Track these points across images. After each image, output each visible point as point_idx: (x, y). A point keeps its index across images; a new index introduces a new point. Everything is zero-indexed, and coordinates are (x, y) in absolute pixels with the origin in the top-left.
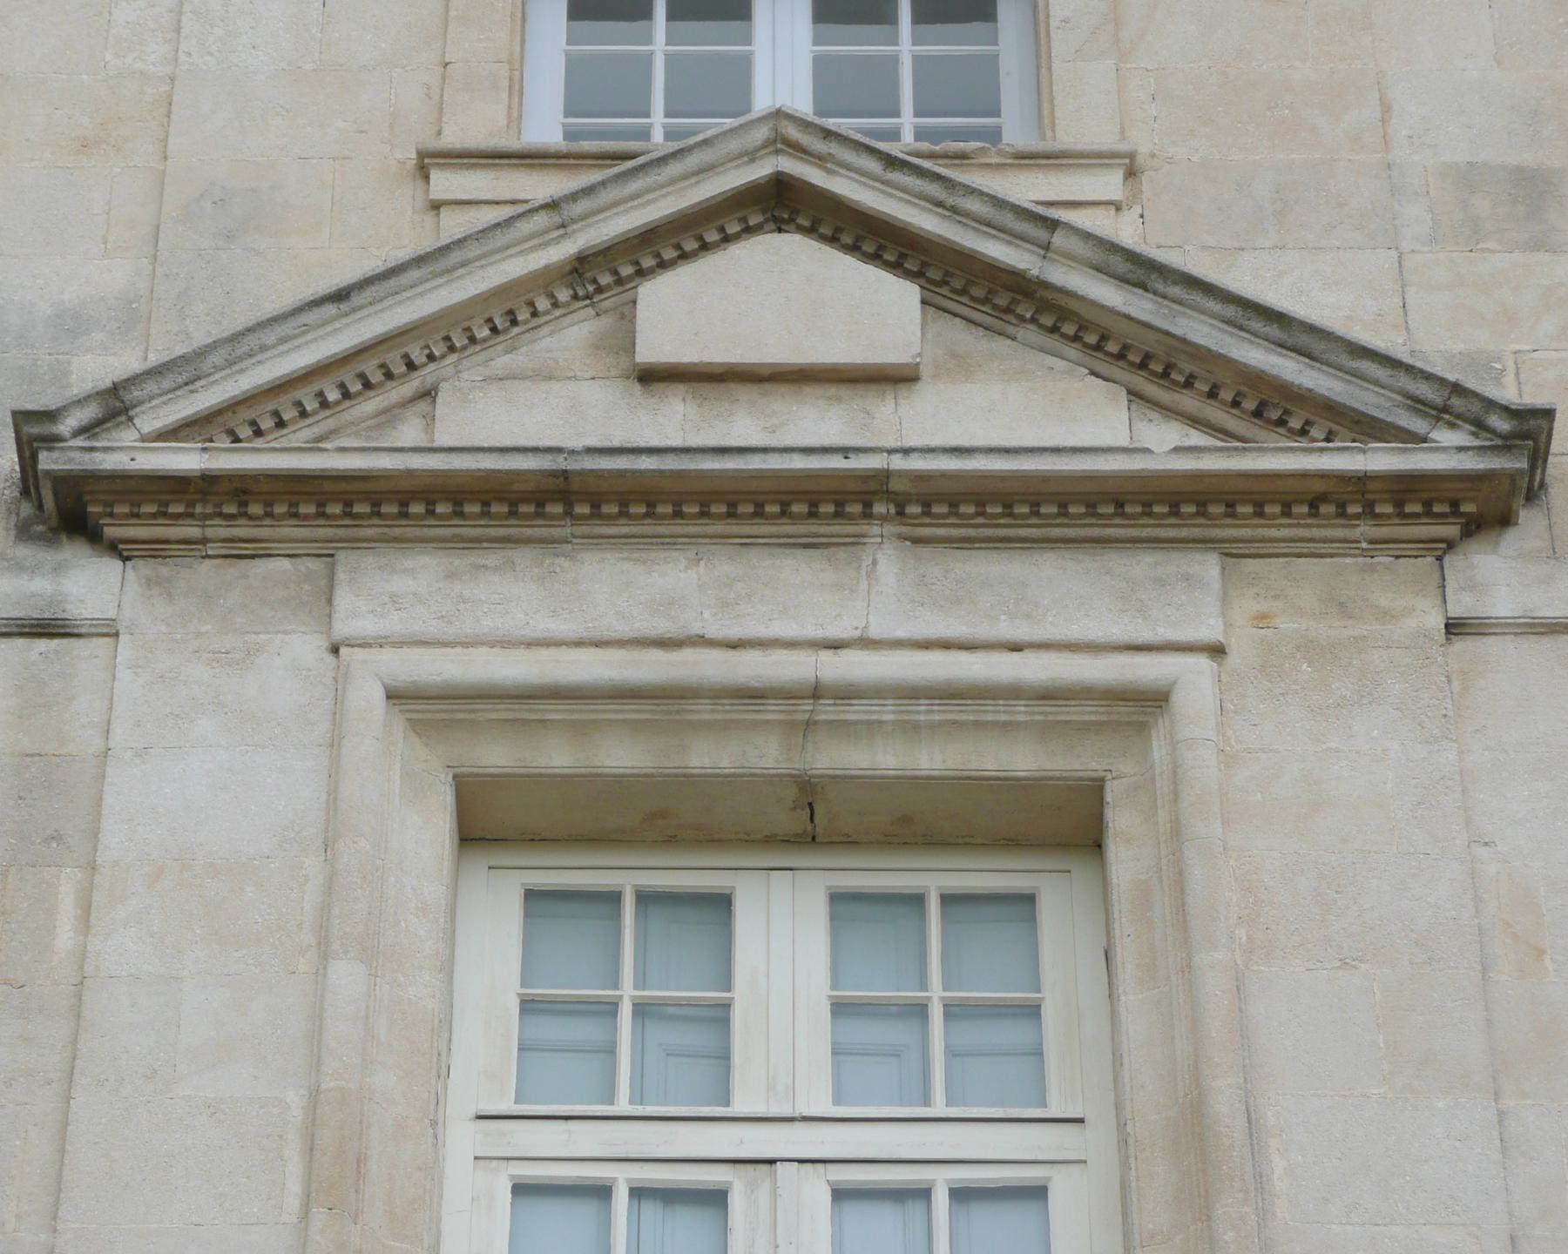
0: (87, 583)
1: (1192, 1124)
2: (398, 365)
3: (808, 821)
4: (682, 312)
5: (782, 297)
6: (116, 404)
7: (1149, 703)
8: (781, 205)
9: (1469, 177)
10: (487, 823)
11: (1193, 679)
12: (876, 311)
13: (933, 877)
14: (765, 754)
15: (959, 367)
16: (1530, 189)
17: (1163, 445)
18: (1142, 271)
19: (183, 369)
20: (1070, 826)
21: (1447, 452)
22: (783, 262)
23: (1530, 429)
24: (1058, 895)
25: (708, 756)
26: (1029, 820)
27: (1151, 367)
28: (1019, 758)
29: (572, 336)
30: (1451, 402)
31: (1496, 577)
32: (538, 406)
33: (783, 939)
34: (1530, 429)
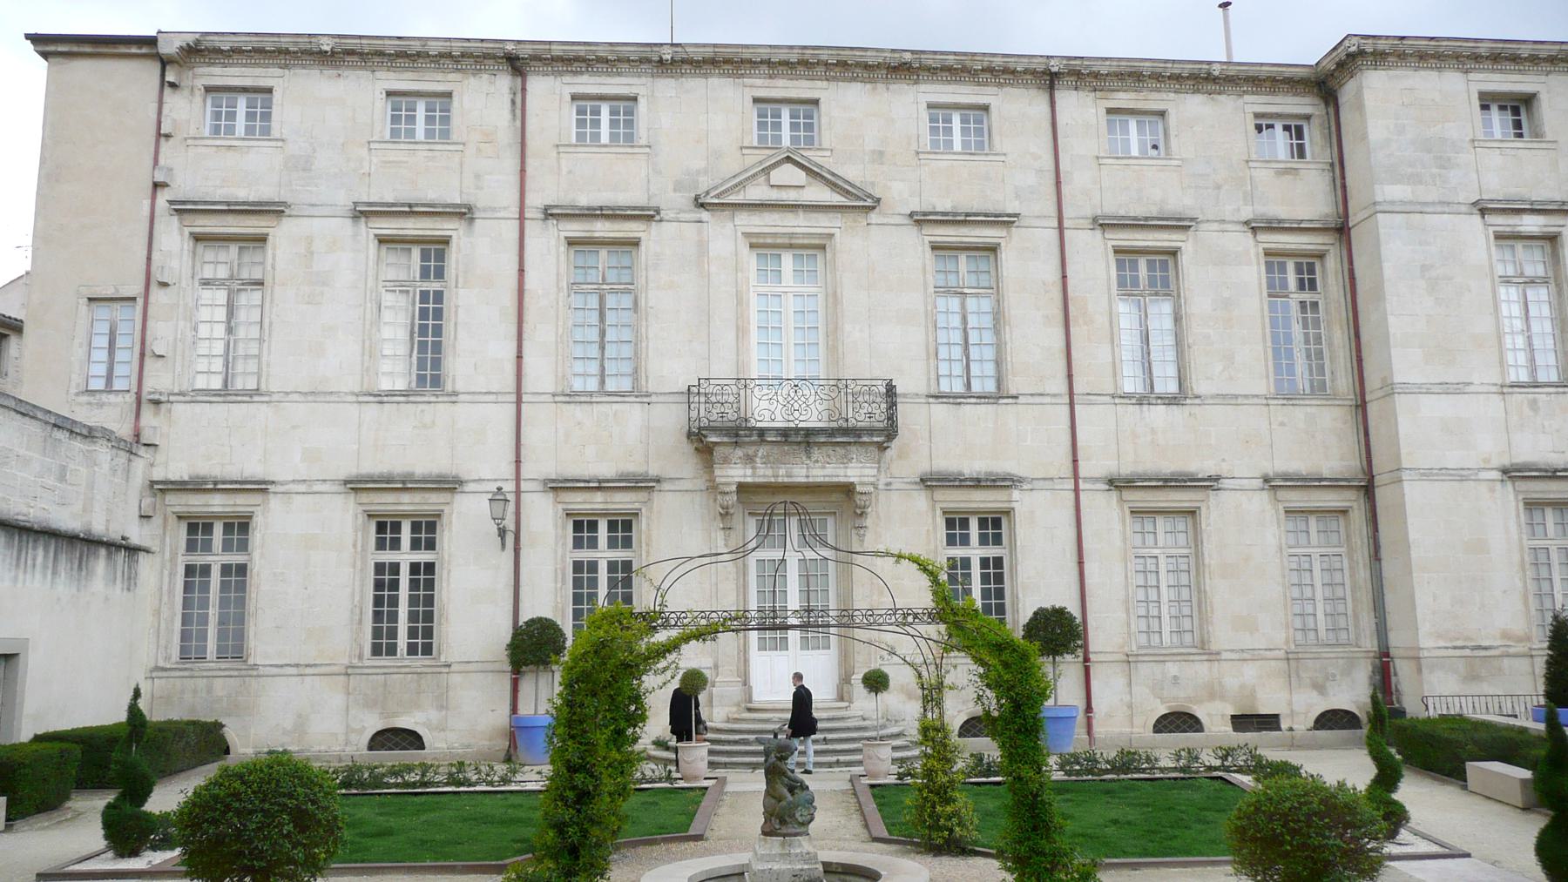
0: (705, 215)
1: (835, 293)
2: (741, 185)
3: (791, 246)
4: (778, 176)
5: (788, 174)
6: (707, 193)
7: (831, 236)
8: (788, 159)
9: (874, 152)
10: (752, 246)
11: (838, 235)
12: (800, 176)
13: (805, 252)
14: (786, 241)
15: (810, 184)
16: (881, 153)
17: (837, 199)
18: (833, 174)
19: (716, 188)
20: (823, 248)
21: (869, 203)
22: (789, 167)
23: (878, 200)
24: (820, 257)
25: (779, 241)
26: (819, 246)
27: (834, 186)
28: (817, 241)
29: (762, 179)
30: (870, 196)
31: (874, 217)
32: (756, 193)
33: (787, 259)
34: (878, 200)
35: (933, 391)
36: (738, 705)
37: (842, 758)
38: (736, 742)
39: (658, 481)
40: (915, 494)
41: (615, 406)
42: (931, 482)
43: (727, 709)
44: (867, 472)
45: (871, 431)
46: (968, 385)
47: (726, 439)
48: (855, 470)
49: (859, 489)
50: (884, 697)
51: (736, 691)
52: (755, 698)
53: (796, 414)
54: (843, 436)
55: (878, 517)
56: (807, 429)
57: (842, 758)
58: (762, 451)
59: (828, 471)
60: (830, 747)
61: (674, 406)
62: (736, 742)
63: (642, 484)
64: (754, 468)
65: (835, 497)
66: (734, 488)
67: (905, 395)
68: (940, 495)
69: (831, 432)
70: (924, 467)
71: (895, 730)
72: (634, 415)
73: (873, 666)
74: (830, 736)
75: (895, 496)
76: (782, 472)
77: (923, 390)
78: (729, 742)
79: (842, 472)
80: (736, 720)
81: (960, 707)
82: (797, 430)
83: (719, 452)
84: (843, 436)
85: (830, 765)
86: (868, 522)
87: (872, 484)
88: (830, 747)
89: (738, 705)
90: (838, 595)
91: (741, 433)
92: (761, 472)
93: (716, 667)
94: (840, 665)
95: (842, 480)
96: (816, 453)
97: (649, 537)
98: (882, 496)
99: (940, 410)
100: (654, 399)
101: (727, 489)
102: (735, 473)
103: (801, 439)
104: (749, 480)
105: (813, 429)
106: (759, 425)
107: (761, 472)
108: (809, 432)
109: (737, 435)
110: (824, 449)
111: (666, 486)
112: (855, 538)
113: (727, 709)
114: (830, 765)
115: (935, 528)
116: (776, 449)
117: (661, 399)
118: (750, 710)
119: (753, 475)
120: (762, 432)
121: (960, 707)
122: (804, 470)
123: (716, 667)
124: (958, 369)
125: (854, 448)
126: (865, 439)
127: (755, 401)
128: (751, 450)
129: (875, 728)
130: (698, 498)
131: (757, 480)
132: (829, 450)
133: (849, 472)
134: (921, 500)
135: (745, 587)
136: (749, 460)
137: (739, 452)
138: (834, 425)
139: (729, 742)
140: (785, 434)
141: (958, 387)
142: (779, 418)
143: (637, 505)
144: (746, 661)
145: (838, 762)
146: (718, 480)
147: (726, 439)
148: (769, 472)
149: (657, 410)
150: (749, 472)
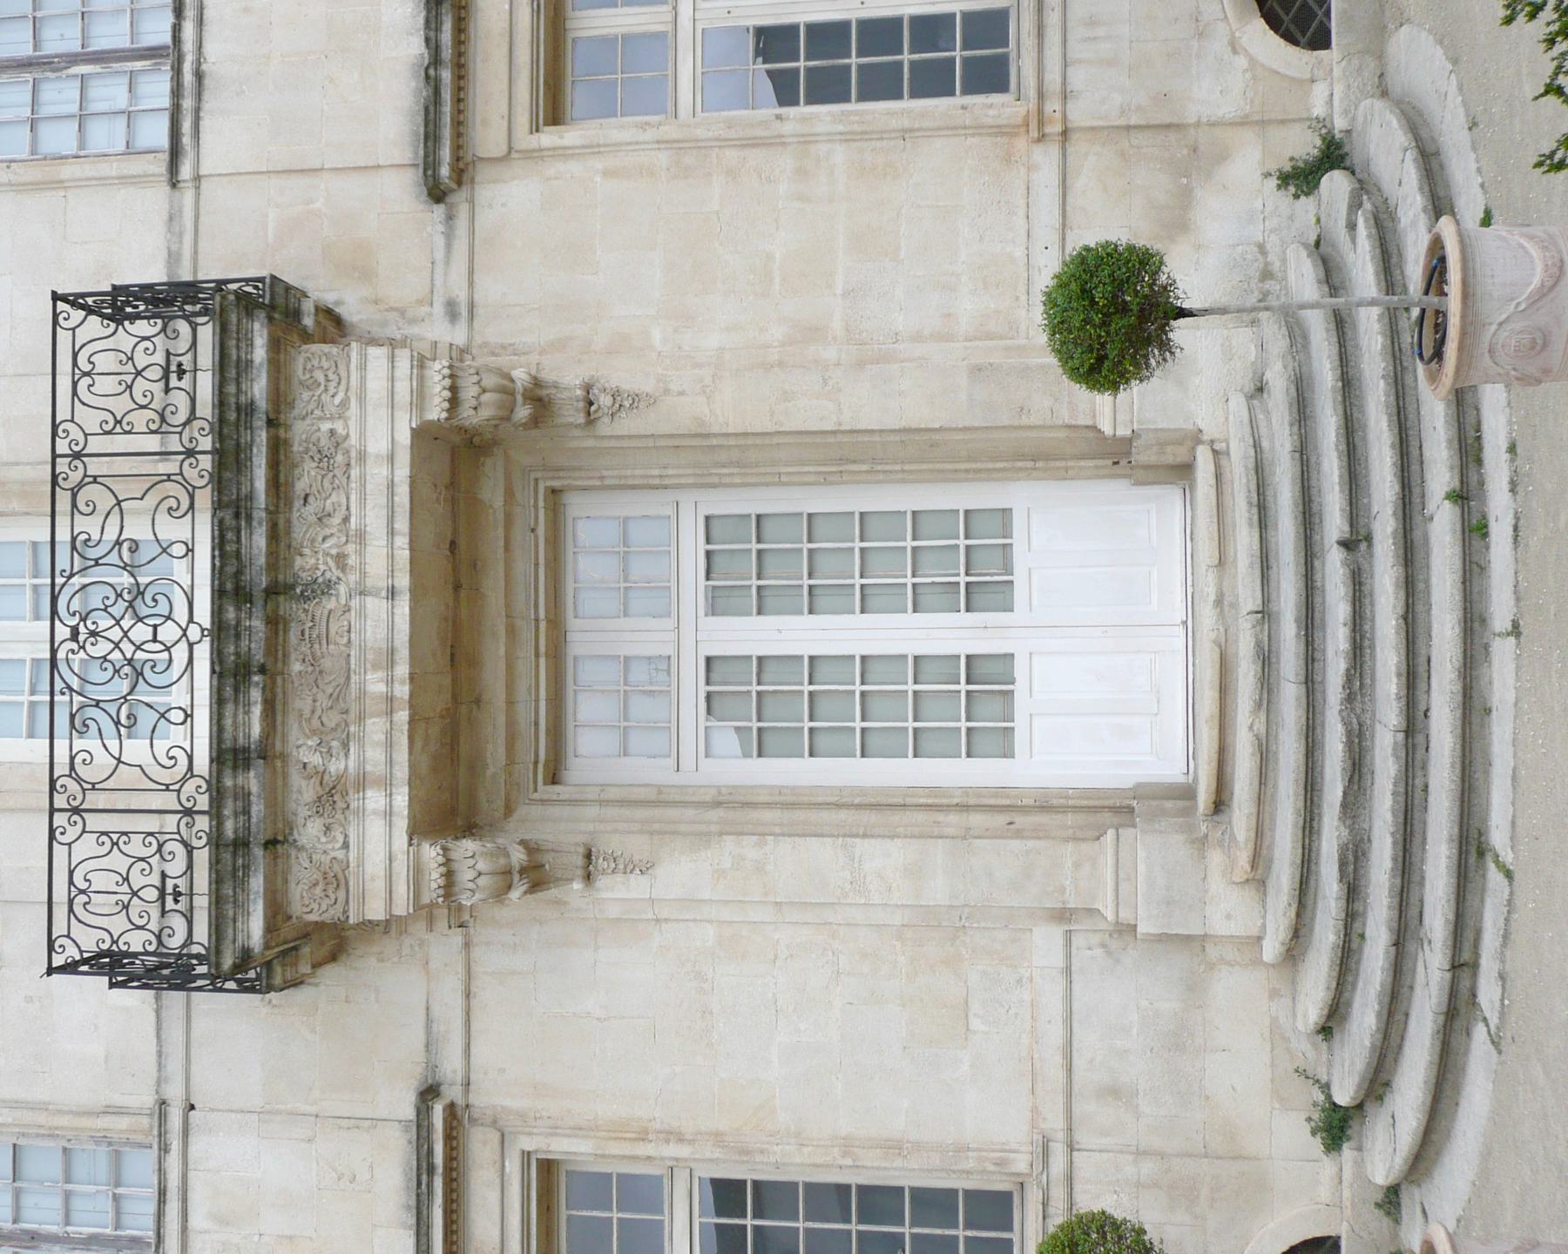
35: (160, 166)
36: (1201, 843)
37: (1440, 476)
38: (1353, 891)
39: (429, 1093)
40: (485, 219)
41: (197, 1221)
42: (446, 168)
43: (1216, 884)
44: (376, 383)
45: (229, 367)
46: (152, 53)
47: (257, 883)
48: (370, 420)
49: (436, 411)
50: (1192, 276)
51: (1151, 852)
52: (1171, 770)
53: (169, 632)
54: (251, 467)
55: (561, 345)
56: (219, 594)
57: (1440, 476)
58: (304, 750)
59: (374, 520)
60: (1384, 526)
61: (200, 1026)
62: (1353, 891)
63: (442, 1137)
64: (362, 783)
65: (492, 493)
66: (431, 853)
67: (173, 258)
68: (488, 136)
69: (231, 512)
70: (399, 190)
71: (1303, 280)
72: (225, 1159)
73: (1032, 322)
74: (1334, 524)
75: (490, 290)
76: (375, 684)
77: (157, 197)
78: (1352, 916)
79: (377, 474)
80: (1260, 858)
81: (1219, 45)
82: (220, 631)
83: (308, 904)
84: (251, 467)
85: (1474, 531)
86: (567, 376)
87: (421, 363)
88: (1384, 526)
89: (1201, 843)
90: (825, 480)
91: (246, 815)
92: (375, 757)
93: (1063, 915)
94: (1064, 475)
95: (403, 472)
96: (310, 563)
97: (618, 1130)
98: (491, 332)
99: (223, 142)
100: (174, 1092)
101: (434, 877)
102: (374, 846)
103: (260, 611)
104: (401, 799)
105: (218, 573)
106: (202, 763)
107: (375, 757)
108: (231, 587)
109: (241, 844)
110: (299, 532)
111: (451, 1066)
112: (628, 424)
113: (1216, 884)
114: (1474, 531)
115: (593, 149)
116: (301, 703)
117: (175, 1066)
118: (1220, 804)
119: (387, 784)
120: (229, 755)
121: (1219, 45)
122: (371, 607)
123: (1063, 915)
124: (110, 92)
125: (299, 431)
126: (259, 388)
127: (126, 776)
128: (303, 791)
129: (1297, 337)
130: (488, 960)
131: (402, 772)
132: (302, 520)
133: (377, 445)
134: (507, 200)
135: (791, 801)
136: (334, 796)
137: (310, 831)
138: (204, 499)
139: (1352, 916)
140: (232, 676)
141: (156, 89)
142: (178, 696)
143: (513, 1167)
144: (1047, 804)
145: (1465, 496)
146: (401, 908)
147: (257, 883)
148: (375, 728)
149: (210, 1082)
150: (374, 799)
